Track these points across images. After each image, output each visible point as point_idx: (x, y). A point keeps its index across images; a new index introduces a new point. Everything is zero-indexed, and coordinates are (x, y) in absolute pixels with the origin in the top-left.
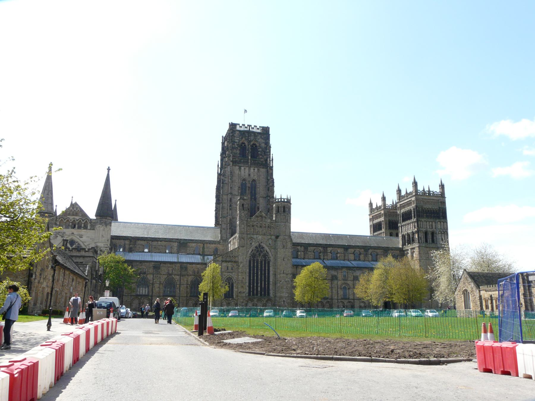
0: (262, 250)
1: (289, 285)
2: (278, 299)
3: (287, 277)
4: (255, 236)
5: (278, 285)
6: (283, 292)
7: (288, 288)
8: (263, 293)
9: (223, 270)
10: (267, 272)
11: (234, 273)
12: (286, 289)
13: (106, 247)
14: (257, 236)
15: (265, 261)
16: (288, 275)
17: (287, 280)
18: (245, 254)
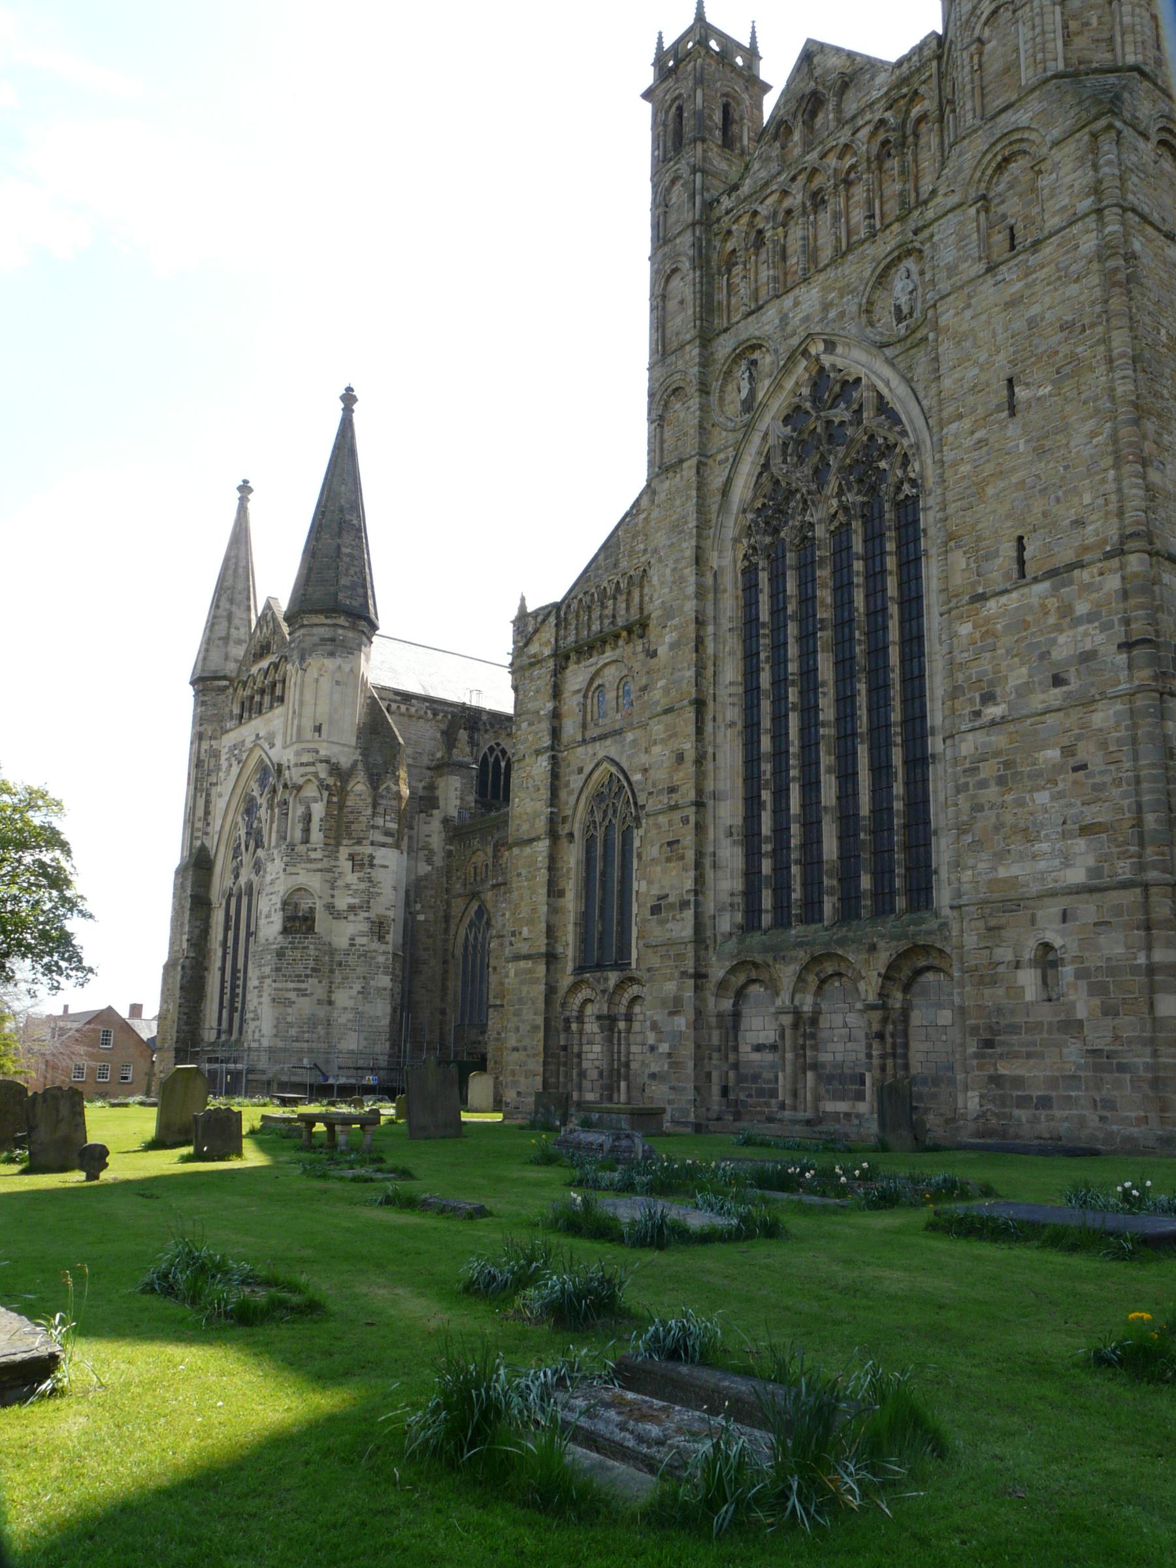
0: (840, 414)
1: (1103, 717)
2: (971, 940)
3: (1066, 611)
4: (771, 313)
5: (967, 746)
6: (1029, 834)
7: (1096, 761)
8: (866, 882)
9: (570, 728)
10: (894, 634)
11: (630, 736)
12: (1065, 781)
13: (307, 764)
14: (788, 302)
15: (871, 516)
16: (1084, 575)
17: (1065, 646)
18: (692, 524)
